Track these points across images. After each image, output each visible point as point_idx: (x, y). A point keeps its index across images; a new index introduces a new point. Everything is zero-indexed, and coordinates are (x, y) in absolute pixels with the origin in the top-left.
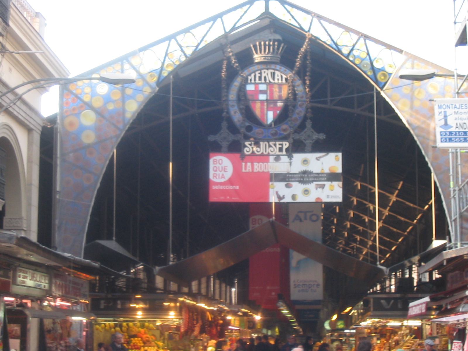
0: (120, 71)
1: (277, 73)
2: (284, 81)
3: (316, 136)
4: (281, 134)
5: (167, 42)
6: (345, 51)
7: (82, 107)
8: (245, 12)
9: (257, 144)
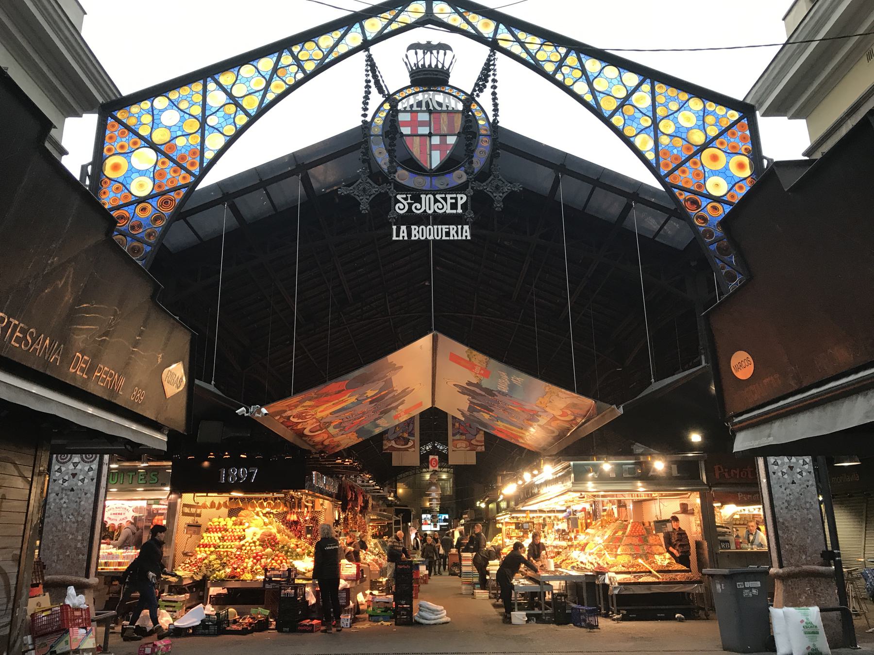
0: (201, 92)
5: (276, 54)
7: (135, 143)
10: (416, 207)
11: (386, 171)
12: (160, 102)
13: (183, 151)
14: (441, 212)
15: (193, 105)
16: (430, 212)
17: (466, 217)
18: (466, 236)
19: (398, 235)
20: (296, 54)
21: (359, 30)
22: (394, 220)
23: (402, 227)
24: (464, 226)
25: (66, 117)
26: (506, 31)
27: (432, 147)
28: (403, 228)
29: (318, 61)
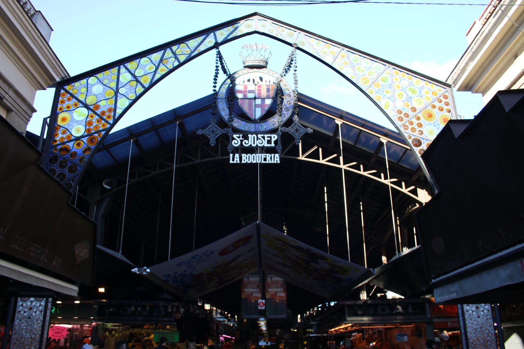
5: (163, 51)
7: (76, 105)
9: (246, 137)
10: (245, 143)
11: (227, 120)
12: (92, 80)
13: (104, 109)
15: (112, 81)
16: (254, 145)
18: (277, 161)
20: (174, 51)
21: (213, 37)
22: (231, 151)
24: (276, 155)
25: (37, 90)
27: (256, 106)
28: (237, 155)
29: (188, 55)
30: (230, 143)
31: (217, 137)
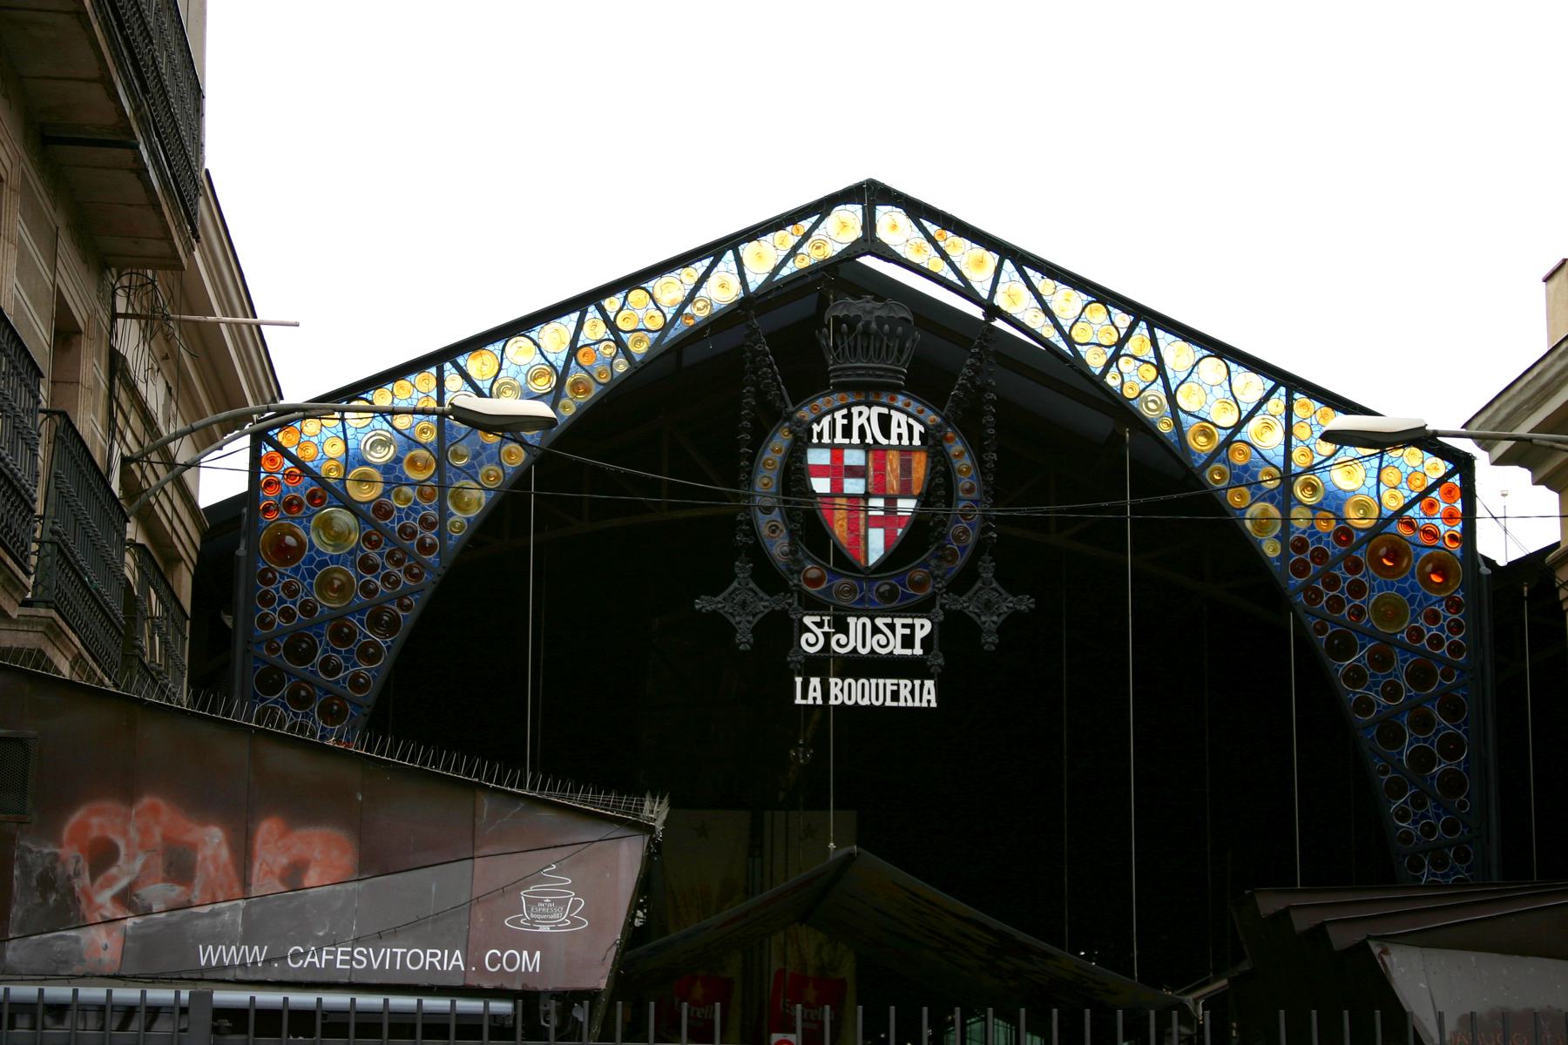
1: (896, 416)
2: (917, 442)
3: (1008, 604)
4: (906, 596)
5: (575, 316)
6: (1095, 360)
8: (807, 236)
11: (784, 568)
14: (883, 651)
16: (864, 651)
17: (929, 663)
18: (929, 701)
19: (805, 696)
21: (733, 267)
23: (812, 679)
24: (926, 682)
26: (1016, 275)
28: (815, 682)
29: (656, 335)
30: (795, 644)
31: (756, 620)
